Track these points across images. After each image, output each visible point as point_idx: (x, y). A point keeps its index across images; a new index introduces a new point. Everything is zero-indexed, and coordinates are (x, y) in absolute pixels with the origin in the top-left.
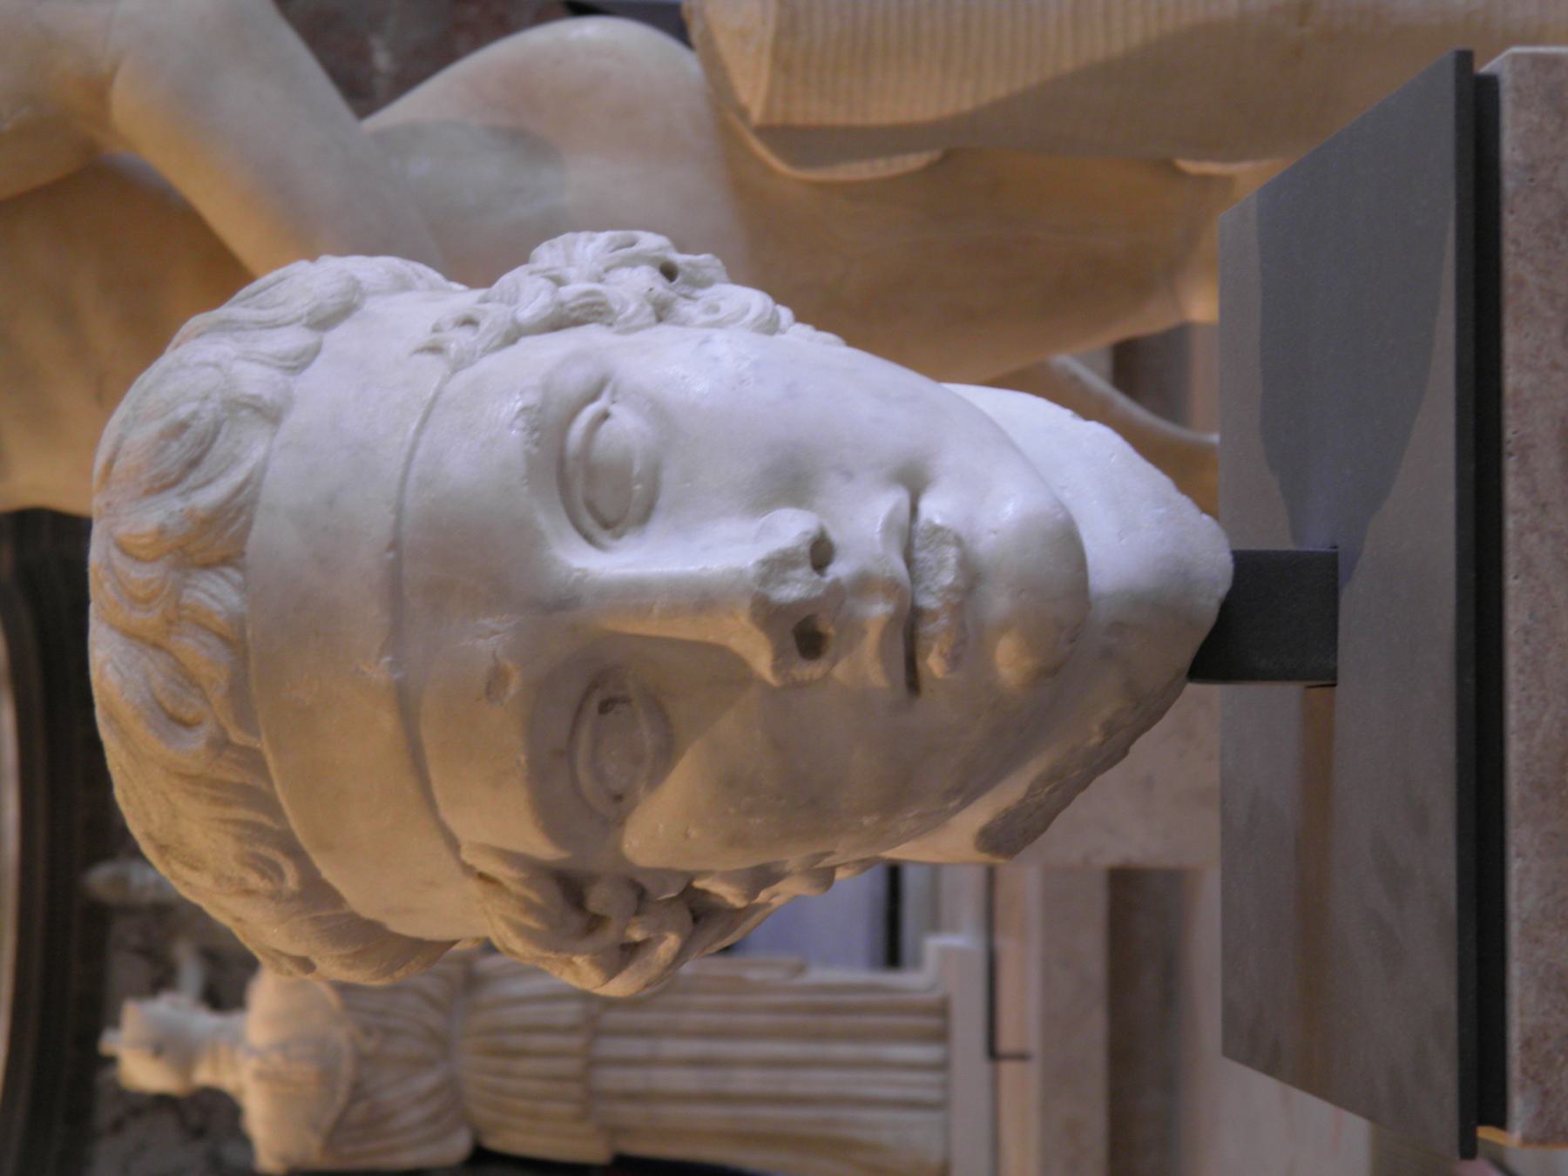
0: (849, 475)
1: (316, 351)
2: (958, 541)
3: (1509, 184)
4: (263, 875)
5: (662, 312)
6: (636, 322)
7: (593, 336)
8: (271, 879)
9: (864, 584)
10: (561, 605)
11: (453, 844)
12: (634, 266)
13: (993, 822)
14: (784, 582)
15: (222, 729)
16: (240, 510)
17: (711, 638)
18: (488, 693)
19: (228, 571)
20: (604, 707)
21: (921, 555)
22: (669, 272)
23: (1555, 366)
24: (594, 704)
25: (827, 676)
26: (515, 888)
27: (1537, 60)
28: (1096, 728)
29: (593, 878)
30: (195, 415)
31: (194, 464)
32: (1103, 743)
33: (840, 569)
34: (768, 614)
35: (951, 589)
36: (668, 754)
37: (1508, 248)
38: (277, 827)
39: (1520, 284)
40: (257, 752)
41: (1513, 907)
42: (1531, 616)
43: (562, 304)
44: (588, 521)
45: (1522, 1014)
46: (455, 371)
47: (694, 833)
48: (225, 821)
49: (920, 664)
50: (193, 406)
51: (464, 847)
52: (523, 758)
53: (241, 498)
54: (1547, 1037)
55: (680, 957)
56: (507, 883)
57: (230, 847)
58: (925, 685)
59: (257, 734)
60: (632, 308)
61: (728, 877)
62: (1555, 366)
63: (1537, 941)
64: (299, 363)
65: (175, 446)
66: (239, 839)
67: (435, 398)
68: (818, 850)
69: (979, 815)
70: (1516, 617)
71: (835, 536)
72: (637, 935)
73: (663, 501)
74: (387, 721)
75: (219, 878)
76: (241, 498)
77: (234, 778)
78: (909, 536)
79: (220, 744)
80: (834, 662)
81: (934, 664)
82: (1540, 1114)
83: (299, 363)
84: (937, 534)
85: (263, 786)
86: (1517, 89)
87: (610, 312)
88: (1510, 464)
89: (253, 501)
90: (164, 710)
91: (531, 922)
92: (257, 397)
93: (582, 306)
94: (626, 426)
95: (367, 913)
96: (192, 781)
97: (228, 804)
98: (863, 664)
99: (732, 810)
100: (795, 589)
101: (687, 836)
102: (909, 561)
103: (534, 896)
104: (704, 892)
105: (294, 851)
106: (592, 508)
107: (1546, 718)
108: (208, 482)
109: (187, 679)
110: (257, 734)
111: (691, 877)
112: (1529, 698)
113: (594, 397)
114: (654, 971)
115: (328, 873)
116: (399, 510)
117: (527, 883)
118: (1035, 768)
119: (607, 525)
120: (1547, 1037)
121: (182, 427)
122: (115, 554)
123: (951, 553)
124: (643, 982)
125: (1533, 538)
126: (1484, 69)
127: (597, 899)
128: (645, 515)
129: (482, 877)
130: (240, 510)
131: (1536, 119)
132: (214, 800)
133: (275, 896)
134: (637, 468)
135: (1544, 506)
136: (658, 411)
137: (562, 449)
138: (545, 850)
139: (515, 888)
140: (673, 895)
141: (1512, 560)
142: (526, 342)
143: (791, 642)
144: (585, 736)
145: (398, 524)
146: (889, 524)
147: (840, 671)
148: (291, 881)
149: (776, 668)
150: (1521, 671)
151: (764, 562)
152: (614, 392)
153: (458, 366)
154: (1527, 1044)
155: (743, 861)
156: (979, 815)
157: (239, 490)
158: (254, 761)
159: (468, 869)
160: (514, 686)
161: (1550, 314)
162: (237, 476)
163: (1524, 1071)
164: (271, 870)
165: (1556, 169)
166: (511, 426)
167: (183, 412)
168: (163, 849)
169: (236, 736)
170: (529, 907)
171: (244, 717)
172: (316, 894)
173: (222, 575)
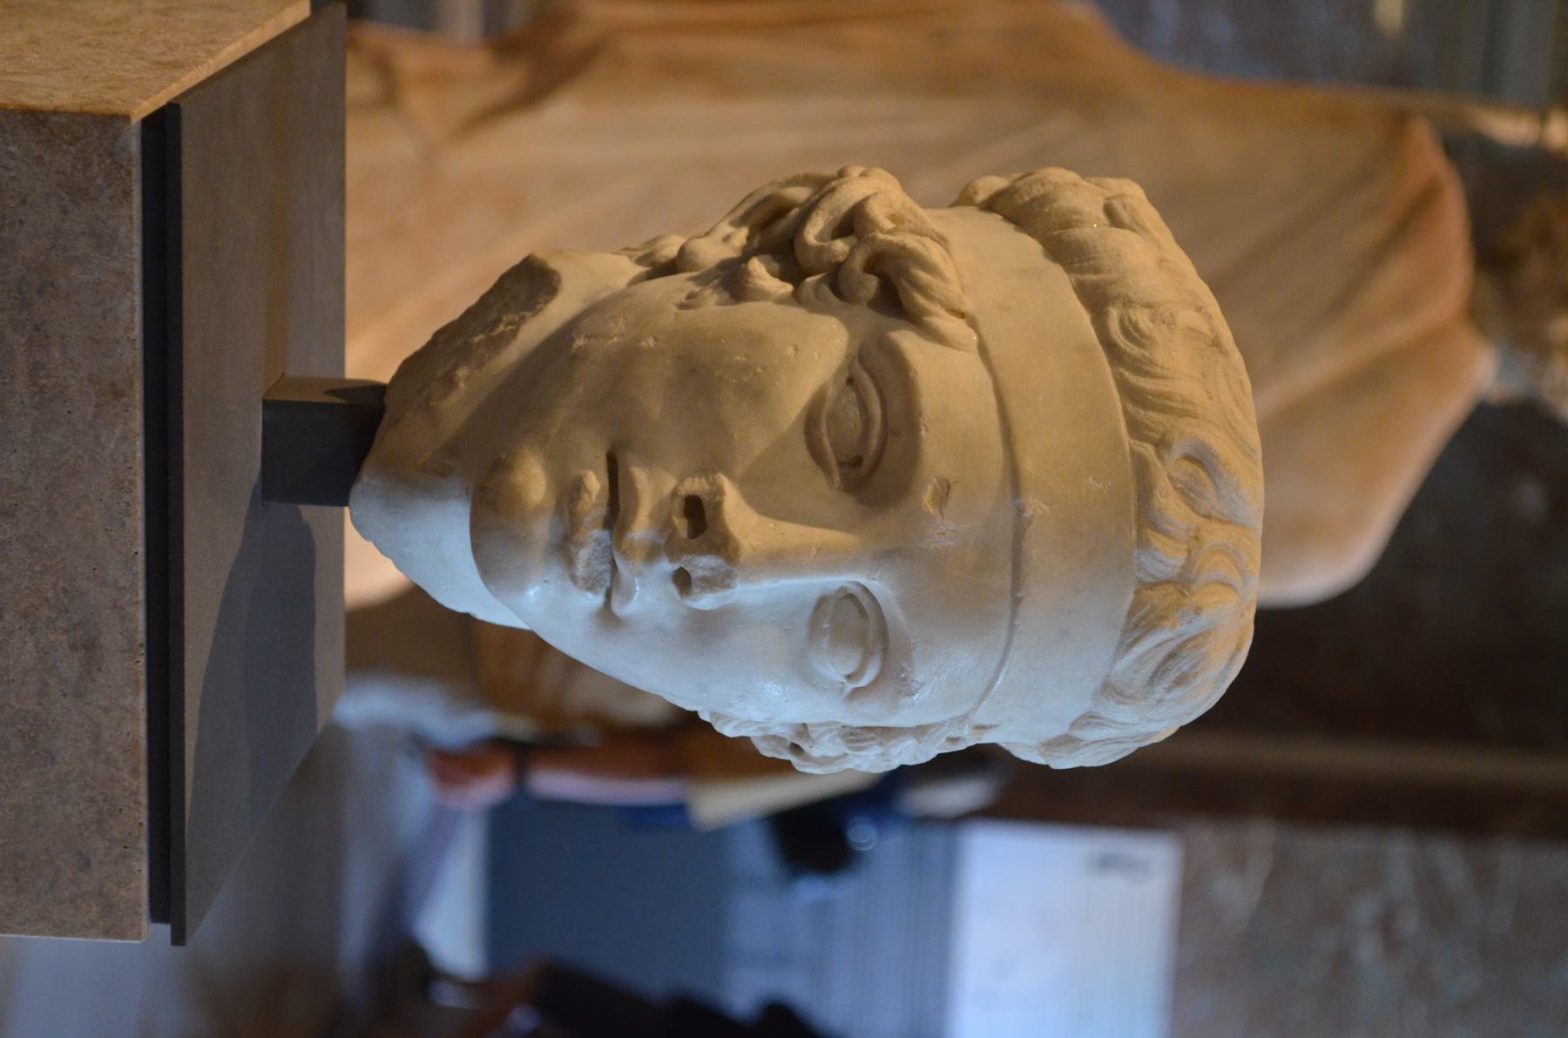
0: (659, 628)
1: (1073, 725)
2: (574, 579)
3: (143, 845)
4: (1136, 327)
5: (803, 730)
6: (822, 730)
7: (857, 722)
8: (1130, 321)
9: (652, 554)
10: (888, 555)
11: (983, 349)
12: (824, 757)
13: (547, 302)
14: (713, 569)
15: (1158, 454)
16: (1136, 626)
17: (771, 524)
18: (949, 486)
19: (1148, 579)
20: (857, 461)
21: (608, 567)
22: (796, 749)
23: (106, 710)
24: (866, 464)
25: (681, 480)
26: (936, 308)
27: (123, 936)
28: (462, 385)
29: (874, 305)
30: (1169, 690)
31: (1172, 656)
32: (456, 367)
33: (667, 566)
34: (723, 546)
35: (581, 545)
36: (811, 420)
37: (143, 798)
38: (1122, 370)
39: (135, 772)
40: (1132, 436)
41: (138, 300)
42: (124, 524)
43: (881, 744)
44: (866, 603)
45: (131, 218)
46: (965, 716)
47: (790, 351)
48: (1164, 377)
49: (606, 482)
50: (1168, 697)
51: (974, 348)
52: (923, 433)
53: (1136, 635)
54: (111, 198)
55: (808, 210)
56: (943, 312)
57: (1160, 356)
58: (602, 462)
59: (1134, 454)
60: (826, 738)
61: (762, 295)
62: (106, 710)
63: (119, 274)
64: (1089, 719)
65: (1185, 668)
66: (1151, 362)
67: (981, 700)
68: (690, 313)
69: (557, 312)
70: (137, 523)
71: (672, 589)
72: (840, 246)
73: (808, 613)
74: (1028, 465)
75: (1171, 323)
76: (1136, 635)
77: (1153, 415)
78: (612, 587)
79: (1162, 445)
80: (674, 493)
81: (595, 483)
82: (116, 138)
83: (1089, 719)
84: (590, 585)
85: (1130, 406)
86: (138, 914)
87: (843, 737)
88: (141, 637)
89: (1126, 631)
90: (1206, 471)
91: (923, 276)
92: (1119, 703)
93: (865, 740)
94: (835, 667)
95: (1056, 270)
96: (1185, 412)
97: (1159, 395)
98: (653, 488)
99: (759, 370)
100: (702, 564)
101: (796, 349)
102: (613, 564)
103: (921, 300)
104: (783, 277)
105: (1109, 345)
106: (862, 612)
107: (112, 446)
108: (1159, 645)
109: (1188, 493)
110: (1134, 454)
111: (796, 298)
112: (126, 461)
113: (856, 690)
114: (826, 205)
115: (1085, 318)
116: (1012, 628)
117: (925, 312)
118: (513, 353)
119: (852, 597)
120: (111, 198)
121: (1179, 682)
122: (1236, 579)
123: (580, 571)
124: (837, 195)
125: (123, 582)
126: (165, 930)
127: (872, 283)
128: (822, 602)
129: (962, 315)
130: (1136, 626)
131: (122, 892)
132: (1169, 397)
133: (1128, 303)
134: (825, 640)
135: (115, 606)
136: (805, 676)
137: (884, 660)
138: (908, 341)
139: (936, 308)
140: (809, 280)
141: (140, 566)
142: (912, 724)
143: (709, 514)
144: (874, 442)
145: (1014, 616)
146: (629, 595)
147: (670, 483)
148: (1114, 314)
149: (720, 492)
150: (132, 482)
151: (728, 586)
152: (842, 690)
153: (963, 719)
154: (127, 194)
155: (748, 312)
156: (557, 312)
157: (1136, 641)
158: (1136, 428)
159: (973, 324)
160: (927, 496)
161: (111, 749)
162: (1139, 650)
163: (129, 173)
164: (1131, 331)
165: (107, 855)
166: (923, 684)
167: (1178, 692)
168: (1216, 343)
169: (1148, 450)
170: (924, 290)
171: (1142, 470)
172: (1096, 299)
173: (1151, 575)
